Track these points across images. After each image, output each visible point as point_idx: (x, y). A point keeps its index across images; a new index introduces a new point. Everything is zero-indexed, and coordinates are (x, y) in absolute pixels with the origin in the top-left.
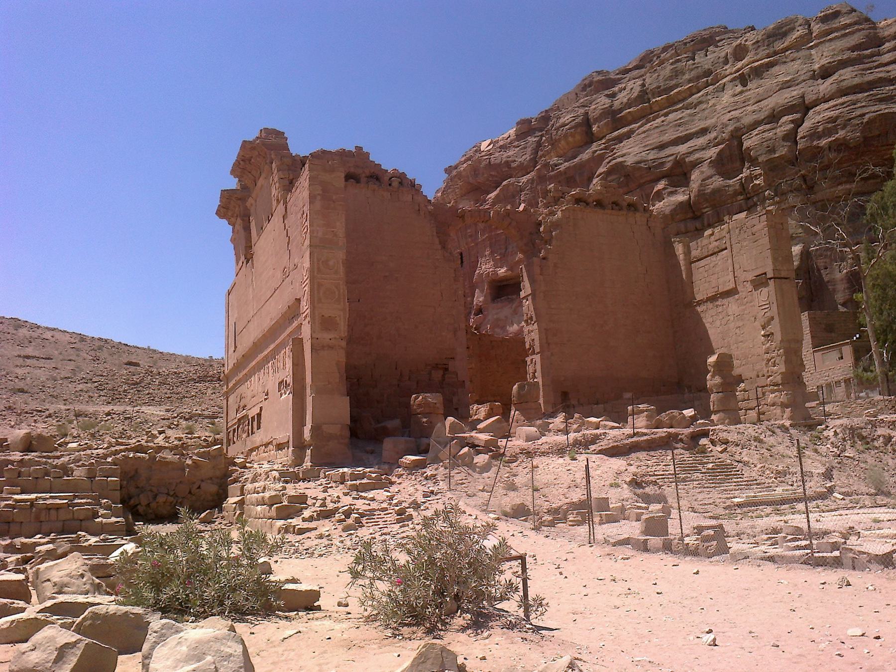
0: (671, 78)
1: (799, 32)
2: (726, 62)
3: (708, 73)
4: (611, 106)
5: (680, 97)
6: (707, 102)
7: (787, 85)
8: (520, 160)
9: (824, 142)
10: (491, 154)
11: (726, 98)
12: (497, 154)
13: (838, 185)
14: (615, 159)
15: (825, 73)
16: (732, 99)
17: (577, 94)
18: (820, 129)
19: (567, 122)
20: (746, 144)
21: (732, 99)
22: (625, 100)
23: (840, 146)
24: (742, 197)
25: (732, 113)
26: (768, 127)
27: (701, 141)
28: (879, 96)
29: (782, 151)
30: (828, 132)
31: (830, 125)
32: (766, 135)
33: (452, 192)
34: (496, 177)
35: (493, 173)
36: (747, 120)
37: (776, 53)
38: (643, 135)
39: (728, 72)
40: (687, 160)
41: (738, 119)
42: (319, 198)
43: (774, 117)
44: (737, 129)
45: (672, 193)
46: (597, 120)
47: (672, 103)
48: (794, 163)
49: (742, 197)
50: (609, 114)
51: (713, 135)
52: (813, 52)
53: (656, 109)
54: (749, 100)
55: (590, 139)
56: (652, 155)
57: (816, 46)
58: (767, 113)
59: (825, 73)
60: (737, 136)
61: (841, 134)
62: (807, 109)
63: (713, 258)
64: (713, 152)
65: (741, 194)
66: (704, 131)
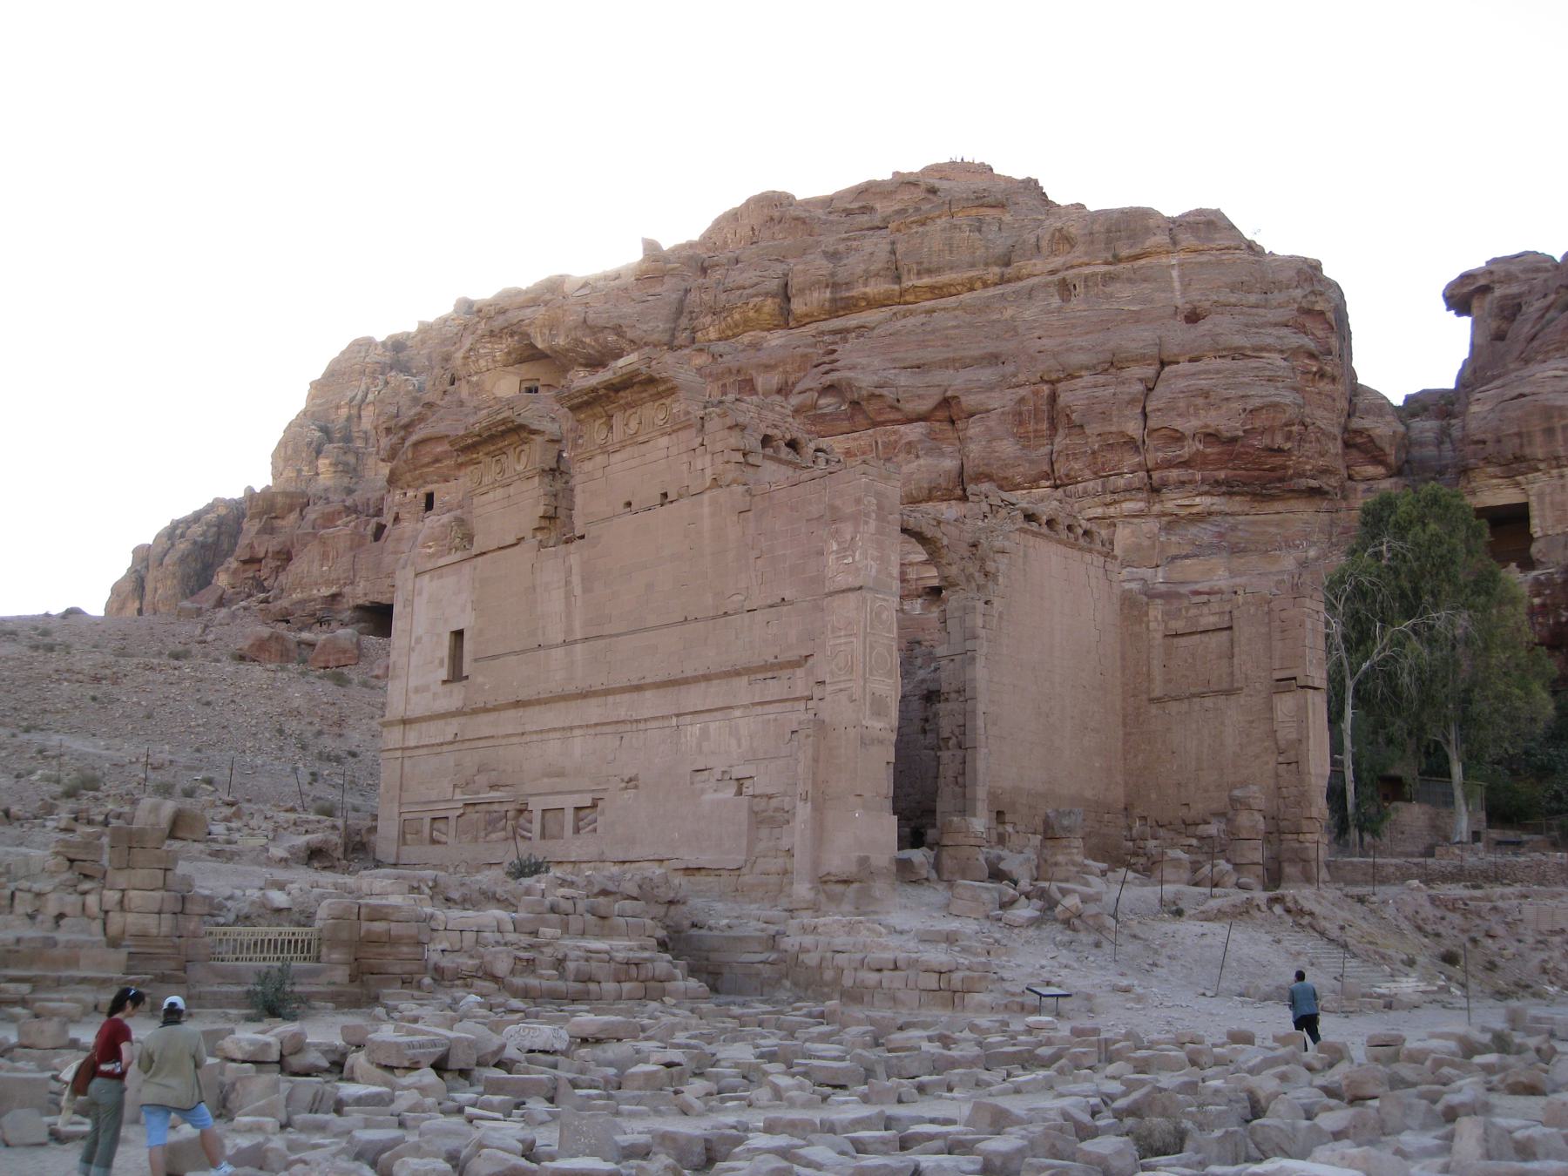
4: (832, 275)
5: (953, 291)
7: (1136, 318)
8: (645, 327)
9: (1188, 425)
13: (1197, 495)
17: (753, 229)
19: (747, 284)
20: (1064, 399)
23: (1211, 437)
24: (1048, 483)
26: (1101, 379)
27: (987, 375)
28: (1268, 373)
31: (1200, 401)
32: (1099, 392)
33: (486, 355)
34: (593, 347)
35: (588, 340)
37: (1117, 260)
38: (887, 340)
40: (963, 399)
42: (874, 515)
43: (1114, 364)
46: (802, 291)
47: (937, 292)
48: (1138, 447)
49: (1048, 483)
50: (827, 286)
53: (909, 298)
54: (1074, 326)
55: (785, 319)
63: (1205, 638)
65: (1048, 479)
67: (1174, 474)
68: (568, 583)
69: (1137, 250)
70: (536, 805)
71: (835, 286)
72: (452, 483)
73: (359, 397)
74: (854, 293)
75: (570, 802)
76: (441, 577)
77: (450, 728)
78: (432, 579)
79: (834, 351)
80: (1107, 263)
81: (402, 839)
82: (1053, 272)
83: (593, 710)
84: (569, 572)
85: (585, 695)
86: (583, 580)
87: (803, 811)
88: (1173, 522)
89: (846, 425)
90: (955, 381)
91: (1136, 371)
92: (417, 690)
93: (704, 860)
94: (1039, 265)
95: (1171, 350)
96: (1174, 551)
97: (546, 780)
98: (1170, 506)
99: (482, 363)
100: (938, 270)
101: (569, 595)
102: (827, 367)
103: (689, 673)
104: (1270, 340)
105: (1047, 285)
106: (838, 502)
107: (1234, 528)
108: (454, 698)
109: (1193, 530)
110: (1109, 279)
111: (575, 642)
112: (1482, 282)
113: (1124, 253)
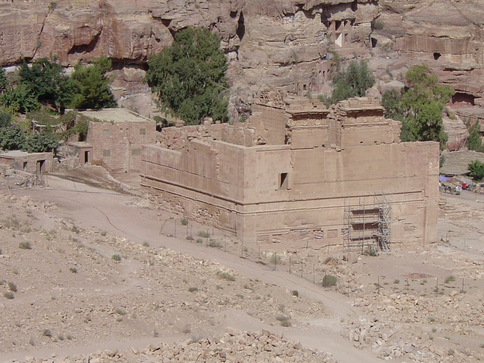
68: (338, 163)
76: (272, 153)
77: (282, 206)
78: (266, 154)
84: (338, 160)
86: (344, 163)
92: (261, 192)
97: (329, 221)
101: (338, 167)
103: (386, 192)
106: (433, 153)
111: (341, 181)
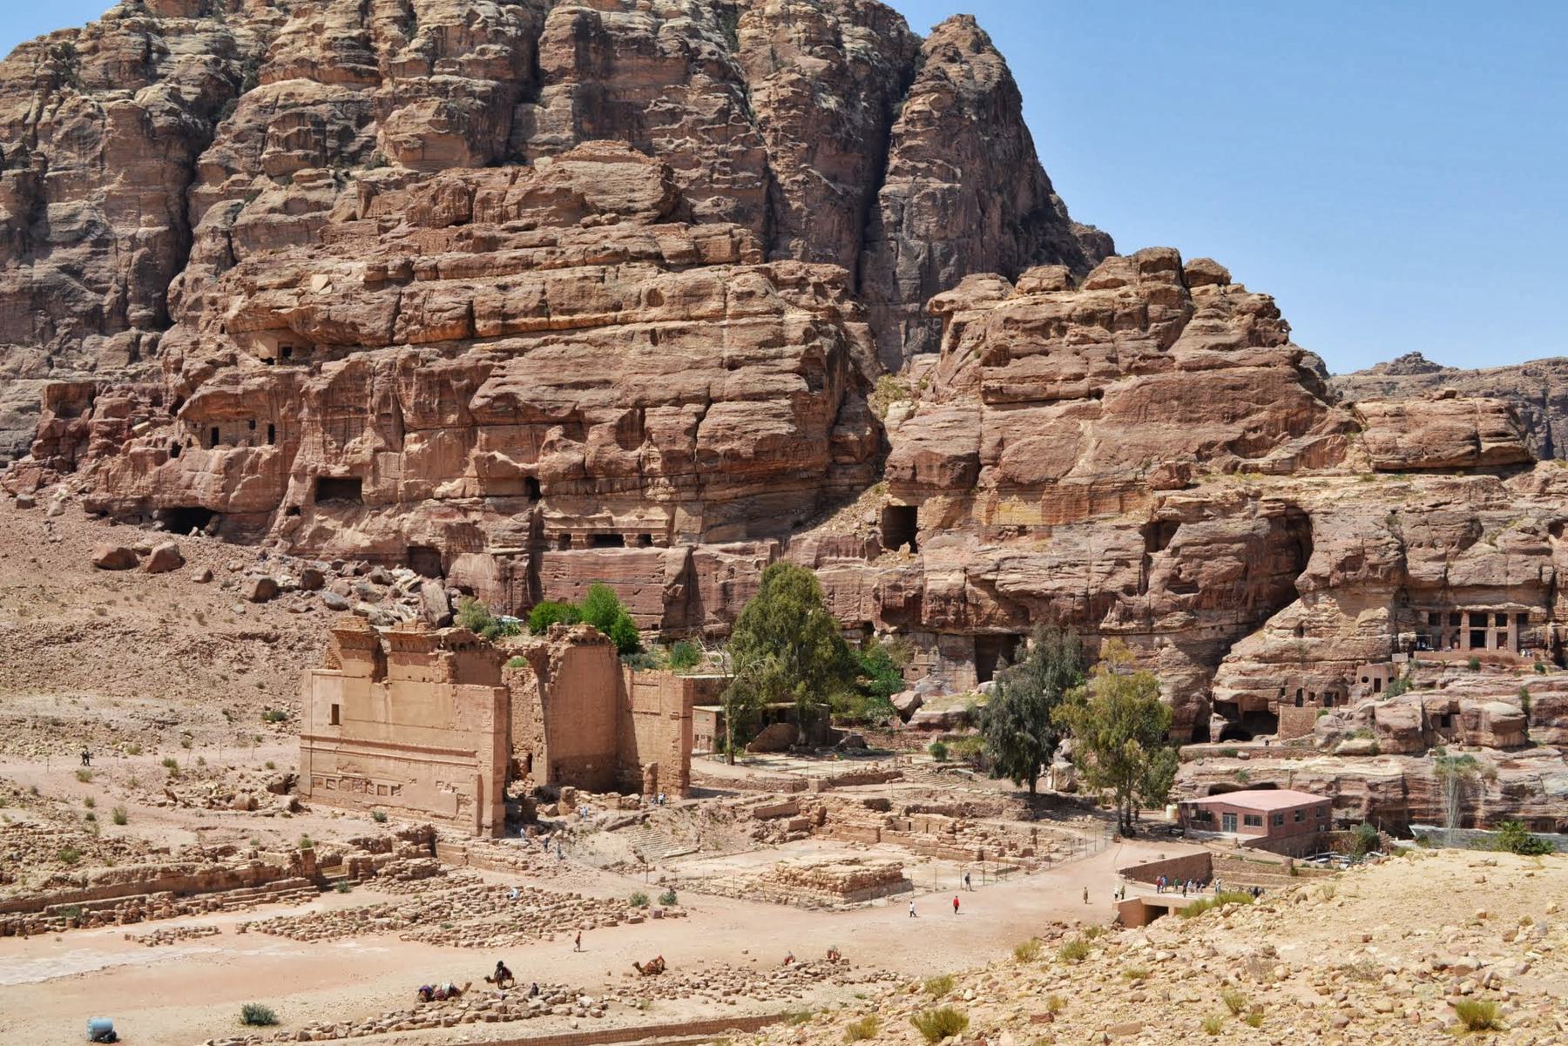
0: (576, 298)
1: (713, 305)
2: (638, 303)
3: (617, 307)
6: (613, 347)
7: (695, 366)
9: (721, 448)
10: (329, 304)
11: (634, 351)
12: (339, 307)
14: (504, 384)
15: (733, 365)
16: (640, 359)
18: (719, 434)
20: (649, 422)
21: (640, 359)
22: (521, 306)
23: (733, 455)
25: (639, 377)
26: (673, 409)
29: (682, 446)
30: (725, 438)
31: (729, 433)
36: (654, 394)
39: (639, 317)
41: (644, 388)
43: (679, 401)
44: (642, 399)
45: (566, 448)
46: (482, 317)
47: (574, 327)
51: (617, 394)
52: (725, 332)
55: (472, 336)
56: (548, 396)
57: (729, 326)
58: (673, 394)
59: (733, 365)
60: (641, 405)
61: (735, 445)
62: (709, 401)
64: (614, 415)
66: (606, 383)
67: (712, 478)
69: (699, 312)
70: (376, 782)
71: (506, 316)
72: (232, 424)
73: (32, 115)
74: (518, 321)
75: (390, 784)
77: (333, 746)
79: (503, 368)
80: (683, 319)
81: (313, 785)
82: (649, 321)
83: (398, 753)
85: (394, 747)
87: (475, 804)
88: (712, 506)
89: (512, 420)
90: (583, 397)
91: (691, 408)
93: (442, 813)
94: (640, 313)
95: (715, 393)
96: (712, 522)
98: (709, 495)
99: (248, 326)
100: (574, 311)
102: (500, 380)
104: (780, 386)
105: (644, 332)
107: (753, 503)
108: (334, 733)
109: (725, 508)
110: (682, 332)
112: (946, 308)
113: (694, 313)
